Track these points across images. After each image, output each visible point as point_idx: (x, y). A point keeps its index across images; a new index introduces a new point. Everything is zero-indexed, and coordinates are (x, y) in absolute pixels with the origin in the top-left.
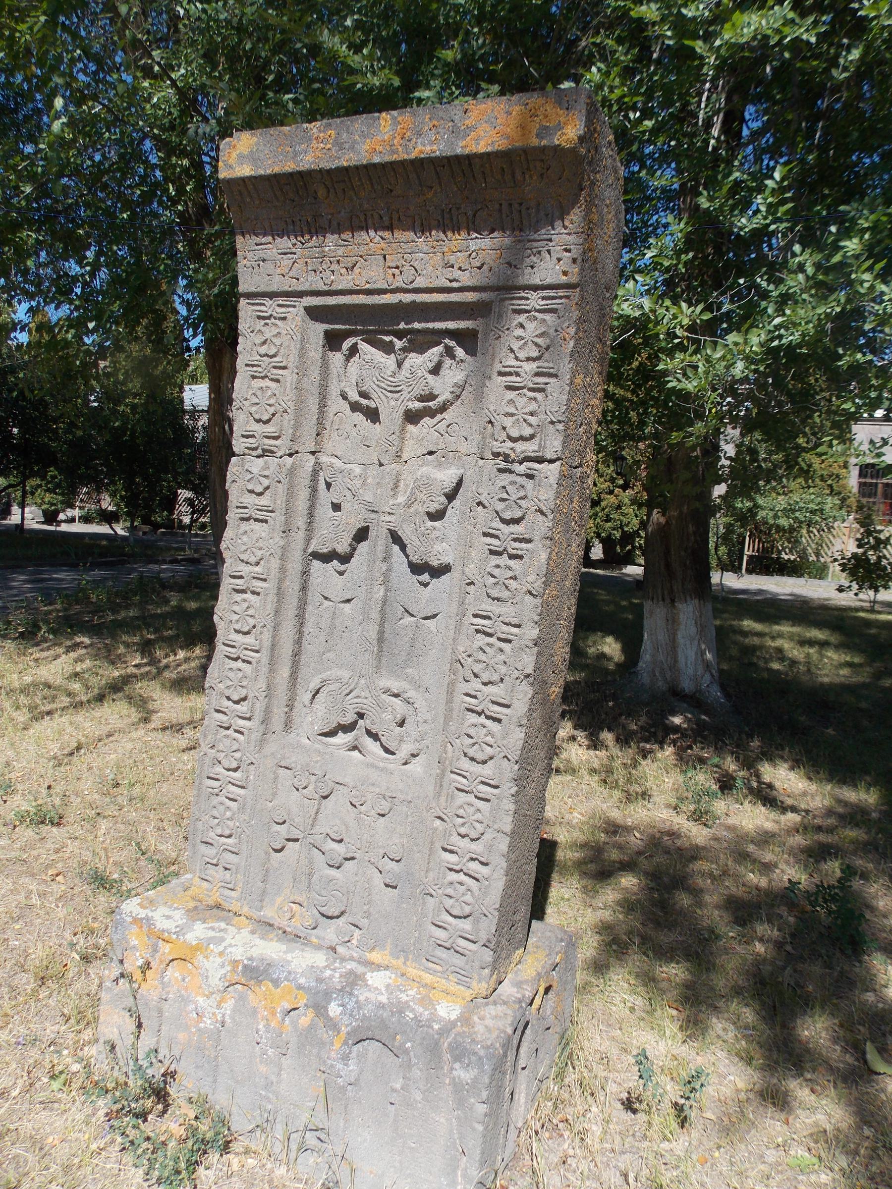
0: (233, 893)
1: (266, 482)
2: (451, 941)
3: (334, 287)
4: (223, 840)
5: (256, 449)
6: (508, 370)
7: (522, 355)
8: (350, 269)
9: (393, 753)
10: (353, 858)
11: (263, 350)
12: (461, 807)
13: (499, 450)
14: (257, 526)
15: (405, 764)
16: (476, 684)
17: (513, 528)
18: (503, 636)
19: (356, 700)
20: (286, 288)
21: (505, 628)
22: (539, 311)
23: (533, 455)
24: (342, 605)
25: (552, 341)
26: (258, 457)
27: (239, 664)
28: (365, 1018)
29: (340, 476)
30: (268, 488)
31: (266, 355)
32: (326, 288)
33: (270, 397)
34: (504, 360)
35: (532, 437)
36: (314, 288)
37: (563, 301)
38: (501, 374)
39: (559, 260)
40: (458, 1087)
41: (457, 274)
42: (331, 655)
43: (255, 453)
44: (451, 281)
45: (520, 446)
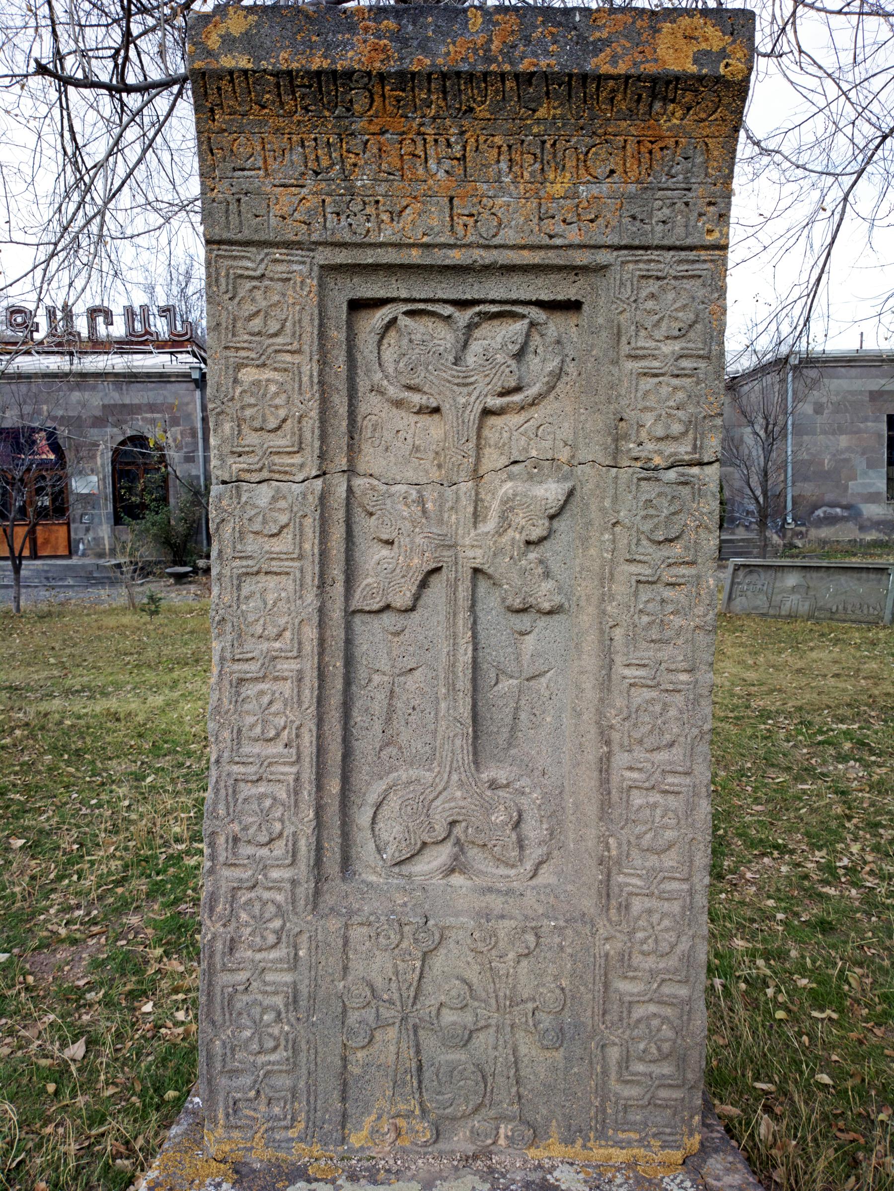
1: (283, 519)
3: (372, 239)
4: (262, 1059)
5: (261, 470)
6: (640, 352)
7: (659, 334)
8: (396, 215)
9: (513, 866)
10: (487, 1027)
11: (256, 324)
14: (271, 582)
15: (531, 878)
16: (639, 754)
18: (671, 687)
21: (671, 677)
23: (687, 457)
24: (402, 678)
25: (697, 316)
27: (262, 789)
29: (388, 501)
30: (286, 526)
31: (259, 334)
32: (357, 239)
34: (633, 341)
35: (685, 434)
36: (338, 238)
37: (705, 266)
38: (629, 356)
39: (701, 215)
41: (560, 228)
42: (392, 750)
43: (256, 477)
44: (551, 237)
45: (670, 448)
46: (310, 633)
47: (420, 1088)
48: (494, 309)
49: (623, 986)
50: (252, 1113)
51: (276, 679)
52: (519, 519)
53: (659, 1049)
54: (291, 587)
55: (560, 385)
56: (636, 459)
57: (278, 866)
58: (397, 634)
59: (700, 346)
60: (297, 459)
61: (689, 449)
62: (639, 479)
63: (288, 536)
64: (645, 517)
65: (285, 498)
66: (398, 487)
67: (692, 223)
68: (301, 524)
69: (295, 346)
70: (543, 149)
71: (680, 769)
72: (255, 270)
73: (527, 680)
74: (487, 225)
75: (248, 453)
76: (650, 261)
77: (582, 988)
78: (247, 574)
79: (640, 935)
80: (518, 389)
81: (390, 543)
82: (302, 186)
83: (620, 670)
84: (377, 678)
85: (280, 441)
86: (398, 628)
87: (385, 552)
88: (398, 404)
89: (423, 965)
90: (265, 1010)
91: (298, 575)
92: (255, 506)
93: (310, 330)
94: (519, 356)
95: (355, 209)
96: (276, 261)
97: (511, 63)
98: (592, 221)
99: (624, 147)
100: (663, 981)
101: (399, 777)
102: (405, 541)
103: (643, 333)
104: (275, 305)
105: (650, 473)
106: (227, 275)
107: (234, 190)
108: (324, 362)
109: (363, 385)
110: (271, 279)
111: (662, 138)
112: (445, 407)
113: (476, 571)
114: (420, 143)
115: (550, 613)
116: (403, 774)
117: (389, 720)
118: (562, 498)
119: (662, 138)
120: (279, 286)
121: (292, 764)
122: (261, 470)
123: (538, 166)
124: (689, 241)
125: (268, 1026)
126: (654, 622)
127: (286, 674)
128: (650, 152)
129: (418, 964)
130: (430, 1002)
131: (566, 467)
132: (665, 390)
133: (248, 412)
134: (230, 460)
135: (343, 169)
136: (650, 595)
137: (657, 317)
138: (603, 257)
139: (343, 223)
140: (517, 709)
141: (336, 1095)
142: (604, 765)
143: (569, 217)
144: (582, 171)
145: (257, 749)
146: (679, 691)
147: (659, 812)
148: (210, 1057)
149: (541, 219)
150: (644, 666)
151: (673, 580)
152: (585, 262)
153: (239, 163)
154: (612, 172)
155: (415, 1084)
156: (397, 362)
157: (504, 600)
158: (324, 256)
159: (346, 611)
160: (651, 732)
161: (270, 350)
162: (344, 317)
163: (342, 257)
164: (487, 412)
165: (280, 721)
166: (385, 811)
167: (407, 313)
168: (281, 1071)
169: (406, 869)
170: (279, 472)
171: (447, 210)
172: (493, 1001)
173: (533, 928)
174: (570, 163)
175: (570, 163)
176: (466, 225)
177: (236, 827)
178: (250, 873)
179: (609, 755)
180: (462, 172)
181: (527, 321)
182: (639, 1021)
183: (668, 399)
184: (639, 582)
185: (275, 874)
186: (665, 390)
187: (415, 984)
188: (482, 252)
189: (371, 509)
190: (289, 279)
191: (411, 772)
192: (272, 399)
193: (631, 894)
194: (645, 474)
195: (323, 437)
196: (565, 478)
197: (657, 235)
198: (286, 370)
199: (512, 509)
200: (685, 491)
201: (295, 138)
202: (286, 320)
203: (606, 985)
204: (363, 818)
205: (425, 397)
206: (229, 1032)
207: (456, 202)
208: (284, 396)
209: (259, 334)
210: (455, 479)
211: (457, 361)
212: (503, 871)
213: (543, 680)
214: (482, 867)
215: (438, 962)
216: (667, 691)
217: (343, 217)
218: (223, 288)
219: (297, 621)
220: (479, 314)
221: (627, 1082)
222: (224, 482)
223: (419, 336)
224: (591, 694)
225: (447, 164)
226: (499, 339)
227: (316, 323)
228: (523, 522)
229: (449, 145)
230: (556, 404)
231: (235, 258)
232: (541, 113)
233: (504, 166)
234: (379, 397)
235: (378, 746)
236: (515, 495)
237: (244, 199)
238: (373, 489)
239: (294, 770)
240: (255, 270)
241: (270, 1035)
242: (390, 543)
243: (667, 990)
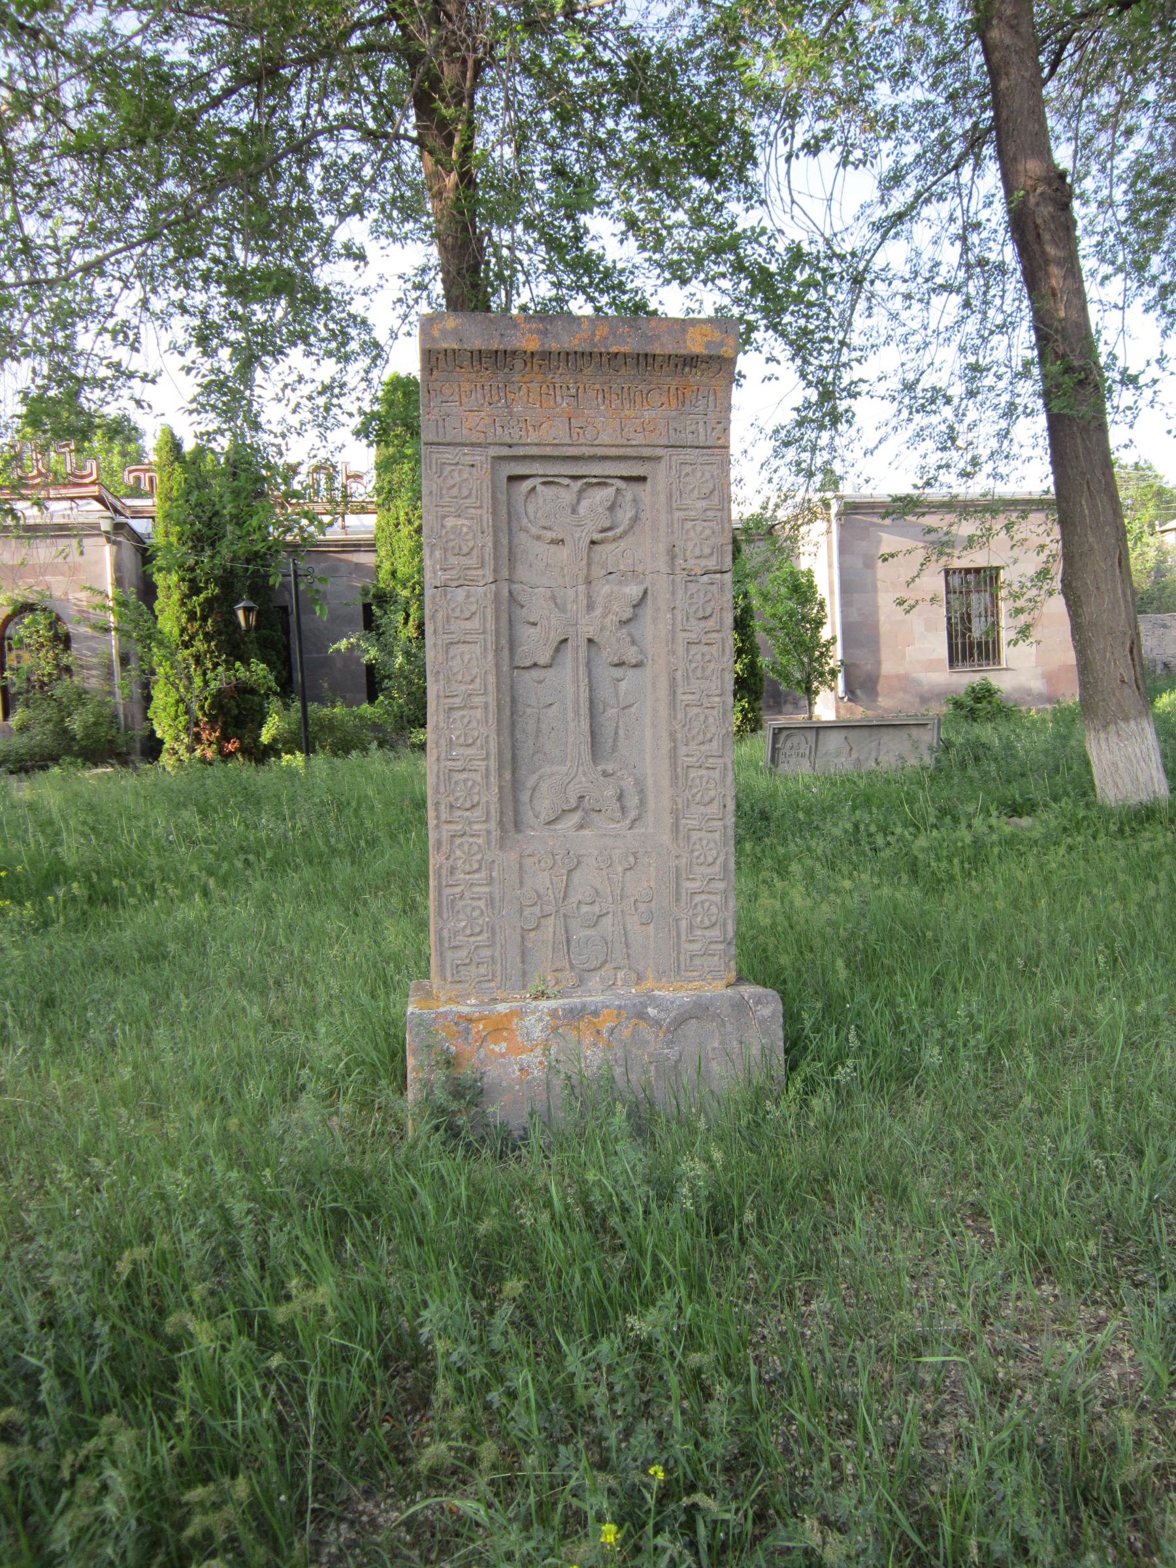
0: (492, 984)
1: (473, 608)
4: (472, 939)
14: (466, 647)
17: (703, 624)
20: (474, 440)
27: (465, 776)
40: (762, 1022)
41: (632, 436)
42: (540, 756)
43: (455, 584)
45: (703, 562)
48: (595, 480)
49: (688, 884)
52: (615, 608)
54: (478, 651)
58: (540, 682)
60: (480, 572)
74: (590, 433)
79: (696, 854)
81: (535, 624)
83: (680, 697)
85: (472, 561)
87: (532, 630)
88: (538, 538)
90: (473, 909)
93: (487, 495)
108: (494, 513)
113: (590, 641)
115: (635, 666)
116: (547, 769)
124: (708, 444)
130: (573, 899)
133: (451, 544)
138: (659, 452)
141: (518, 959)
142: (673, 754)
145: (461, 750)
158: (493, 451)
163: (505, 452)
164: (593, 542)
174: (638, 400)
175: (638, 400)
177: (451, 799)
179: (675, 748)
185: (476, 827)
186: (699, 529)
195: (496, 558)
196: (641, 583)
197: (690, 439)
200: (714, 588)
203: (678, 884)
204: (525, 797)
213: (633, 710)
215: (577, 876)
224: (663, 711)
232: (623, 371)
233: (600, 400)
242: (535, 624)
243: (713, 885)
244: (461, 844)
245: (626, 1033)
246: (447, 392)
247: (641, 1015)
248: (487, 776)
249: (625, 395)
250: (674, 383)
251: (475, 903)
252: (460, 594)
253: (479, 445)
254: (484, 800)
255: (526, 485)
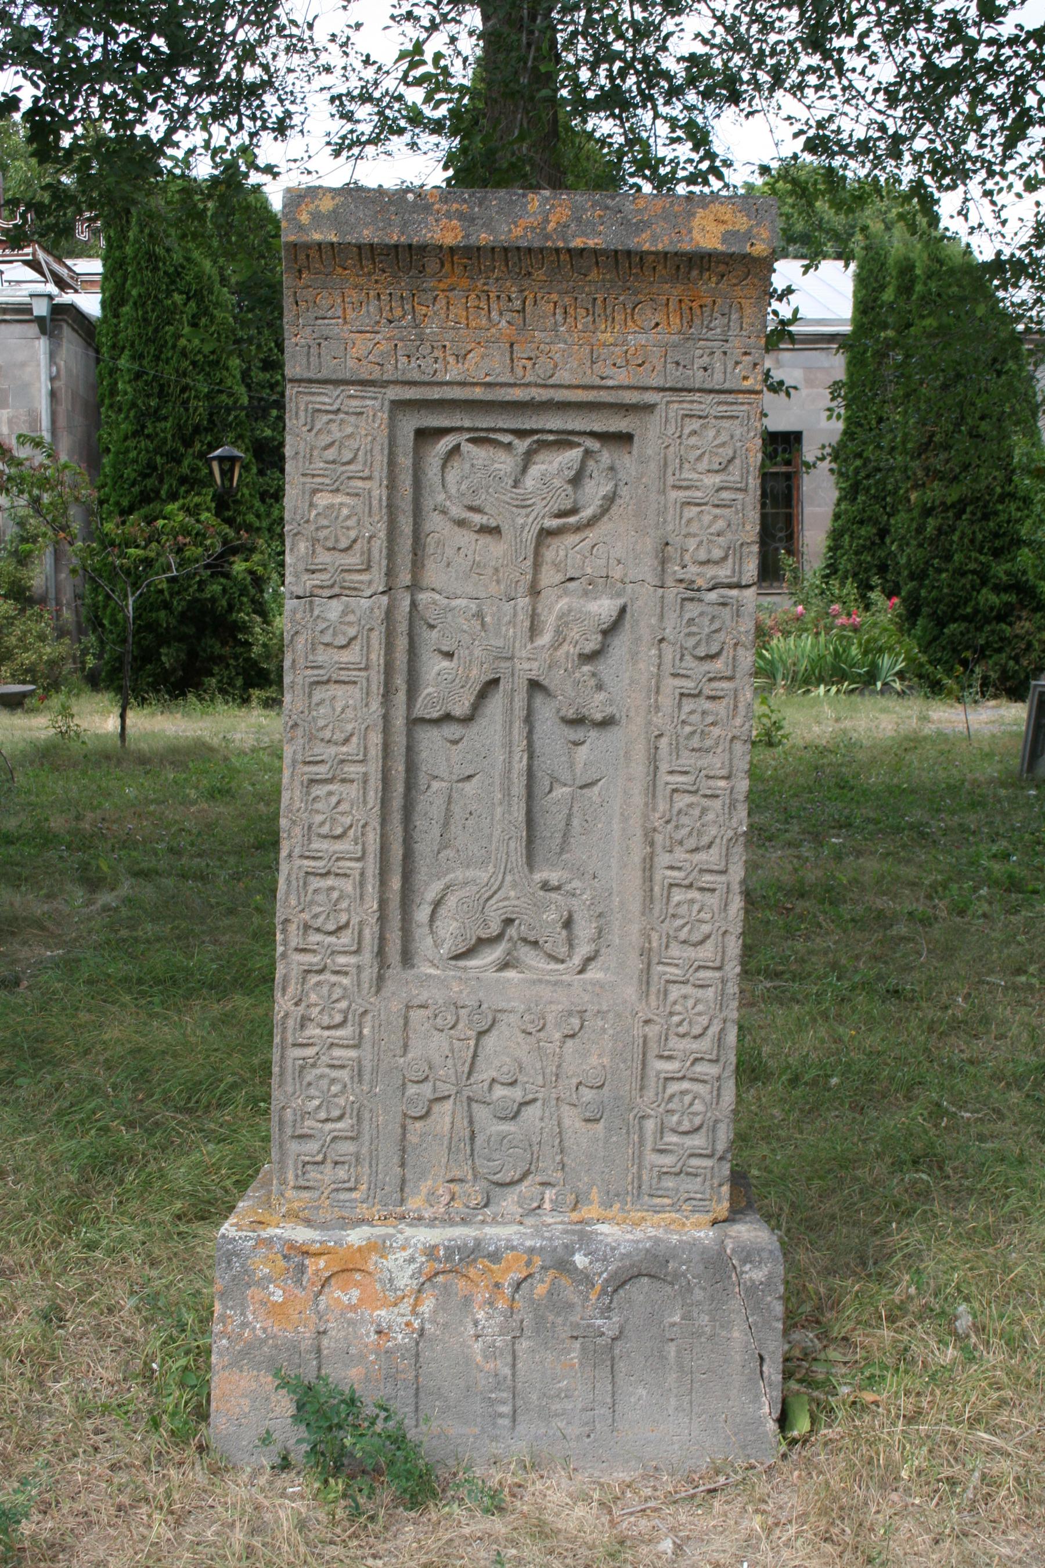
0: (354, 1195)
1: (352, 632)
2: (680, 1164)
3: (439, 377)
4: (329, 1126)
5: (332, 586)
6: (685, 484)
9: (563, 962)
10: (534, 1100)
11: (331, 454)
12: (675, 1003)
13: (682, 577)
14: (339, 691)
15: (580, 972)
17: (707, 666)
18: (709, 792)
19: (501, 904)
20: (365, 376)
21: (711, 783)
22: (716, 417)
24: (460, 785)
26: (330, 598)
27: (330, 882)
28: (623, 1256)
29: (449, 615)
30: (355, 638)
31: (334, 462)
32: (426, 378)
33: (348, 517)
34: (677, 472)
35: (725, 558)
36: (408, 377)
38: (674, 487)
39: (737, 363)
40: (751, 1290)
41: (610, 371)
42: (449, 853)
43: (327, 593)
45: (711, 571)
46: (376, 739)
47: (472, 1155)
48: (551, 438)
50: (319, 1176)
51: (343, 781)
52: (574, 634)
53: (691, 1121)
54: (358, 695)
55: (614, 508)
56: (681, 581)
57: (345, 953)
58: (455, 742)
59: (738, 479)
61: (729, 573)
62: (684, 600)
63: (356, 647)
64: (689, 634)
65: (353, 612)
66: (458, 602)
67: (729, 370)
68: (368, 637)
69: (367, 473)
70: (594, 306)
71: (716, 868)
72: (331, 405)
73: (581, 788)
74: (544, 366)
75: (320, 570)
76: (692, 402)
77: (622, 1065)
78: (318, 683)
79: (676, 1019)
80: (573, 511)
82: (377, 333)
83: (664, 778)
84: (436, 785)
85: (353, 560)
86: (457, 737)
87: (445, 663)
88: (461, 523)
89: (477, 1045)
90: (333, 1081)
91: (365, 684)
92: (325, 619)
93: (380, 460)
94: (576, 481)
95: (425, 353)
96: (351, 397)
97: (565, 240)
98: (640, 365)
99: (667, 305)
100: (696, 1060)
101: (456, 878)
102: (463, 652)
103: (686, 466)
104: (349, 436)
105: (692, 592)
106: (306, 410)
107: (315, 336)
108: (392, 486)
109: (428, 503)
110: (347, 413)
111: (700, 297)
112: (505, 528)
114: (484, 297)
116: (459, 875)
117: (446, 824)
118: (615, 614)
119: (700, 297)
120: (352, 419)
121: (358, 860)
122: (332, 586)
123: (590, 318)
124: (727, 386)
125: (335, 1096)
126: (694, 732)
127: (352, 776)
128: (691, 309)
129: (472, 1043)
131: (619, 585)
132: (707, 519)
133: (322, 534)
134: (305, 577)
135: (414, 318)
136: (692, 707)
137: (699, 452)
139: (413, 365)
140: (570, 816)
141: (396, 1160)
142: (649, 865)
143: (619, 362)
144: (630, 323)
145: (325, 845)
146: (717, 796)
147: (696, 907)
148: (281, 1123)
149: (593, 363)
150: (686, 773)
151: (713, 693)
152: (634, 401)
153: (321, 313)
154: (657, 325)
155: (468, 1152)
156: (458, 483)
157: (558, 711)
158: (394, 393)
159: (407, 718)
160: (690, 834)
161: (343, 477)
162: (411, 444)
165: (347, 820)
166: (443, 911)
167: (468, 440)
168: (346, 1138)
169: (461, 963)
170: (349, 588)
171: (508, 354)
172: (540, 1078)
173: (579, 1012)
174: (619, 317)
176: (525, 367)
177: (306, 916)
178: (319, 957)
179: (652, 856)
180: (521, 322)
181: (582, 449)
182: (672, 1096)
183: (709, 527)
184: (682, 695)
185: (342, 960)
186: (707, 519)
187: (469, 1060)
188: (541, 391)
189: (432, 622)
190: (362, 413)
191: (467, 874)
192: (344, 521)
193: (668, 982)
194: (690, 594)
195: (391, 555)
196: (619, 595)
197: (699, 379)
198: (357, 495)
199: (566, 624)
200: (726, 612)
201: (372, 293)
202: (358, 449)
204: (422, 915)
205: (486, 517)
206: (299, 1101)
207: (515, 347)
208: (355, 519)
209: (334, 462)
210: (513, 595)
211: (516, 484)
212: (553, 966)
213: (596, 789)
214: (533, 963)
215: (490, 1041)
216: (705, 796)
217: (413, 360)
218: (302, 421)
219: (363, 727)
220: (537, 441)
221: (661, 1151)
222: (298, 597)
223: (480, 462)
224: (638, 800)
225: (508, 316)
226: (556, 465)
227: (386, 452)
228: (577, 637)
229: (510, 300)
230: (611, 525)
231: (314, 394)
232: (593, 275)
233: (559, 318)
234: (441, 516)
235: (436, 849)
236: (570, 611)
237: (324, 343)
238: (434, 603)
239: (358, 865)
240: (331, 405)
241: (337, 1105)
242: (449, 655)
243: (699, 1068)
244: (318, 984)
245: (541, 1289)
246: (325, 303)
247: (563, 1265)
248: (362, 884)
249: (598, 310)
250: (676, 291)
251: (335, 1074)
252: (334, 610)
253: (371, 383)
254: (355, 921)
255: (445, 444)
